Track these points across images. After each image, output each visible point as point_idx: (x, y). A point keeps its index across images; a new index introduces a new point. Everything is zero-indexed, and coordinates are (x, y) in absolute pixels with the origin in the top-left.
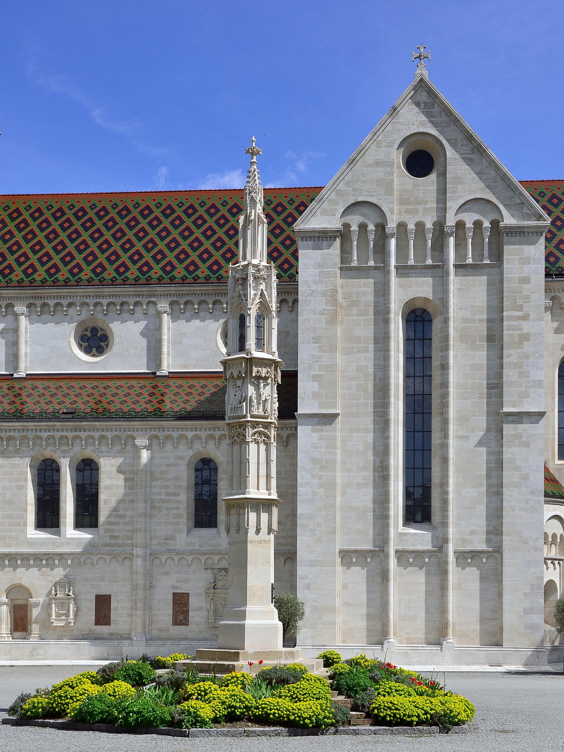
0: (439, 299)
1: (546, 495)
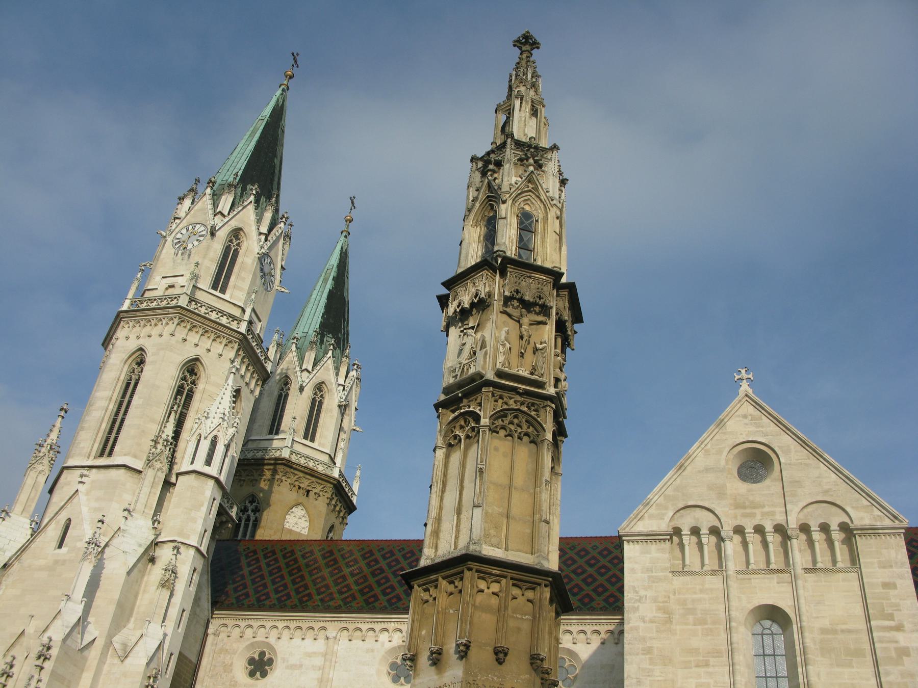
0: (789, 607)
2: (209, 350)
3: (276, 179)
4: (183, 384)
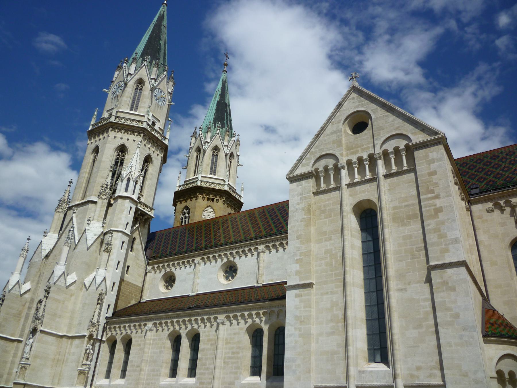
0: (376, 198)
1: (485, 336)
2: (128, 140)
3: (162, 51)
4: (118, 158)
